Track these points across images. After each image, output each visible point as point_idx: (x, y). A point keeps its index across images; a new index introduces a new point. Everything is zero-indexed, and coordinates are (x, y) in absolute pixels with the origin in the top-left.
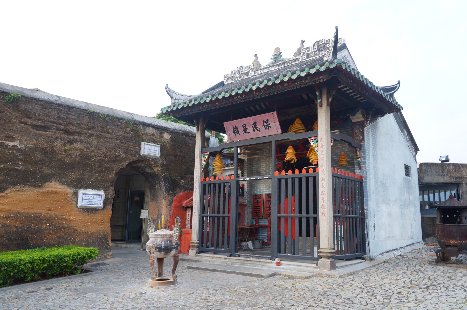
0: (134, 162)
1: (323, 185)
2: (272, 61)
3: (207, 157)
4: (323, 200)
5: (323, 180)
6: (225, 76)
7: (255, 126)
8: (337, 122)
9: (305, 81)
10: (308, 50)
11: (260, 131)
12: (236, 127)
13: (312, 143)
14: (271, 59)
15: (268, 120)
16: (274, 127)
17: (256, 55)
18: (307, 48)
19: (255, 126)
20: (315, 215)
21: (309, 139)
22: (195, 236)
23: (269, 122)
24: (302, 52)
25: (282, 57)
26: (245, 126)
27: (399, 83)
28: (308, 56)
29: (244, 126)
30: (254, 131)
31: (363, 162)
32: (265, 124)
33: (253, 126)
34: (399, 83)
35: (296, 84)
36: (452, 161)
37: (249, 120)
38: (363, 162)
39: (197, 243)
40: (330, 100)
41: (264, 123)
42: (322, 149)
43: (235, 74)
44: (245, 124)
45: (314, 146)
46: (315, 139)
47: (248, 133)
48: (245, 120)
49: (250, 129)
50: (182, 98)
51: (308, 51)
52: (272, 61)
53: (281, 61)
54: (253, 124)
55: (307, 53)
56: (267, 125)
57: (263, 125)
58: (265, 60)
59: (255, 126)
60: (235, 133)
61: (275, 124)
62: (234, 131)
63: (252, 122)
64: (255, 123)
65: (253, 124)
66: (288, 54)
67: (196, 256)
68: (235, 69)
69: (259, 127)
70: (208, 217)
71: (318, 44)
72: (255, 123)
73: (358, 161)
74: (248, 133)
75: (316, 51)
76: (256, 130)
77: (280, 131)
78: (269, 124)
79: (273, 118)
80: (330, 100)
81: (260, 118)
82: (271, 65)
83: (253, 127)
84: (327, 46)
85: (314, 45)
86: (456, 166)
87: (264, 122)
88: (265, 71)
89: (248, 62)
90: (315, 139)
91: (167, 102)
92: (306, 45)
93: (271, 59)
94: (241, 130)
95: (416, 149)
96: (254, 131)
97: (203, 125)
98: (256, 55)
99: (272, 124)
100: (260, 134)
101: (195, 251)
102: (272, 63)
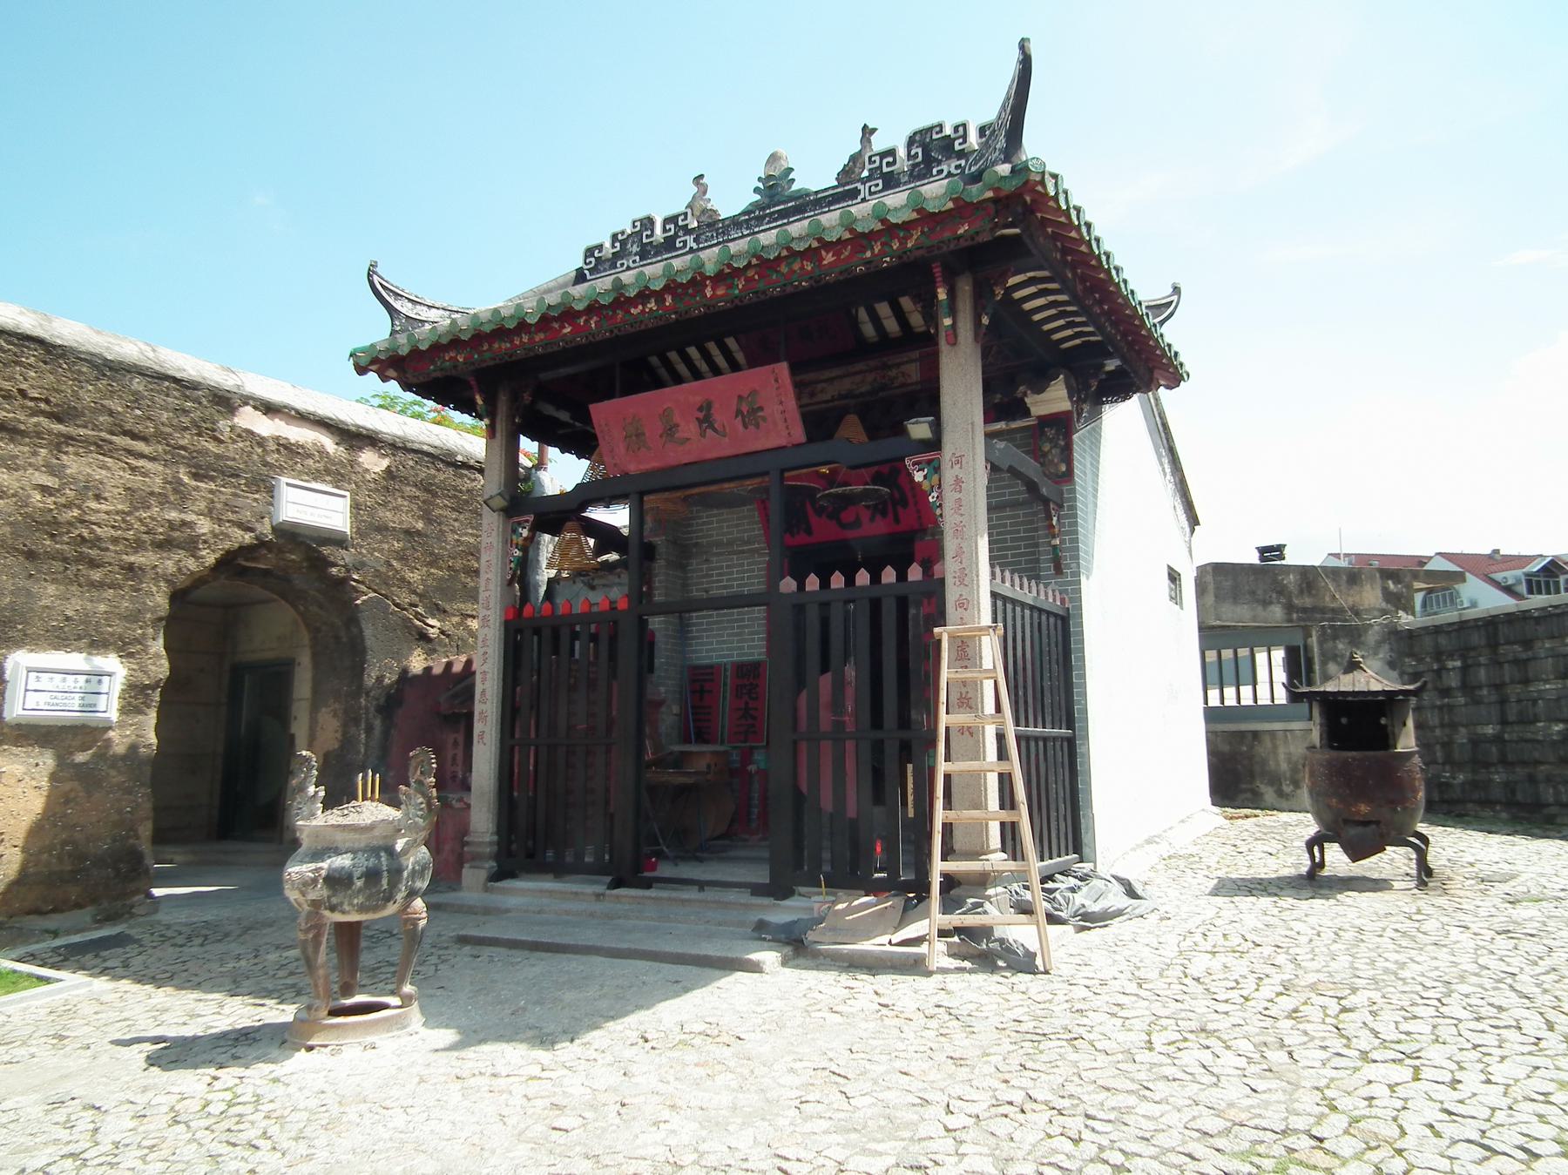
0: (244, 550)
2: (758, 197)
6: (589, 252)
7: (706, 420)
8: (1002, 403)
9: (903, 241)
13: (918, 477)
14: (756, 190)
17: (701, 176)
18: (883, 155)
20: (905, 735)
21: (907, 462)
22: (482, 821)
24: (868, 166)
25: (795, 187)
27: (1176, 290)
30: (703, 435)
31: (1069, 550)
32: (745, 408)
33: (701, 415)
34: (1176, 290)
35: (868, 254)
36: (1292, 558)
38: (1069, 550)
39: (490, 843)
40: (985, 320)
42: (958, 495)
45: (926, 486)
51: (888, 164)
52: (758, 197)
53: (791, 199)
54: (700, 409)
55: (885, 169)
56: (751, 415)
57: (739, 412)
58: (733, 196)
63: (698, 399)
65: (700, 409)
66: (815, 173)
67: (486, 890)
69: (719, 418)
72: (706, 408)
73: (1055, 547)
77: (799, 435)
78: (761, 409)
80: (985, 320)
81: (723, 389)
83: (700, 422)
84: (957, 147)
85: (911, 142)
86: (1308, 576)
90: (929, 462)
91: (376, 330)
92: (879, 144)
93: (756, 190)
95: (1194, 521)
96: (703, 435)
97: (511, 417)
98: (701, 176)
101: (483, 875)
102: (756, 205)
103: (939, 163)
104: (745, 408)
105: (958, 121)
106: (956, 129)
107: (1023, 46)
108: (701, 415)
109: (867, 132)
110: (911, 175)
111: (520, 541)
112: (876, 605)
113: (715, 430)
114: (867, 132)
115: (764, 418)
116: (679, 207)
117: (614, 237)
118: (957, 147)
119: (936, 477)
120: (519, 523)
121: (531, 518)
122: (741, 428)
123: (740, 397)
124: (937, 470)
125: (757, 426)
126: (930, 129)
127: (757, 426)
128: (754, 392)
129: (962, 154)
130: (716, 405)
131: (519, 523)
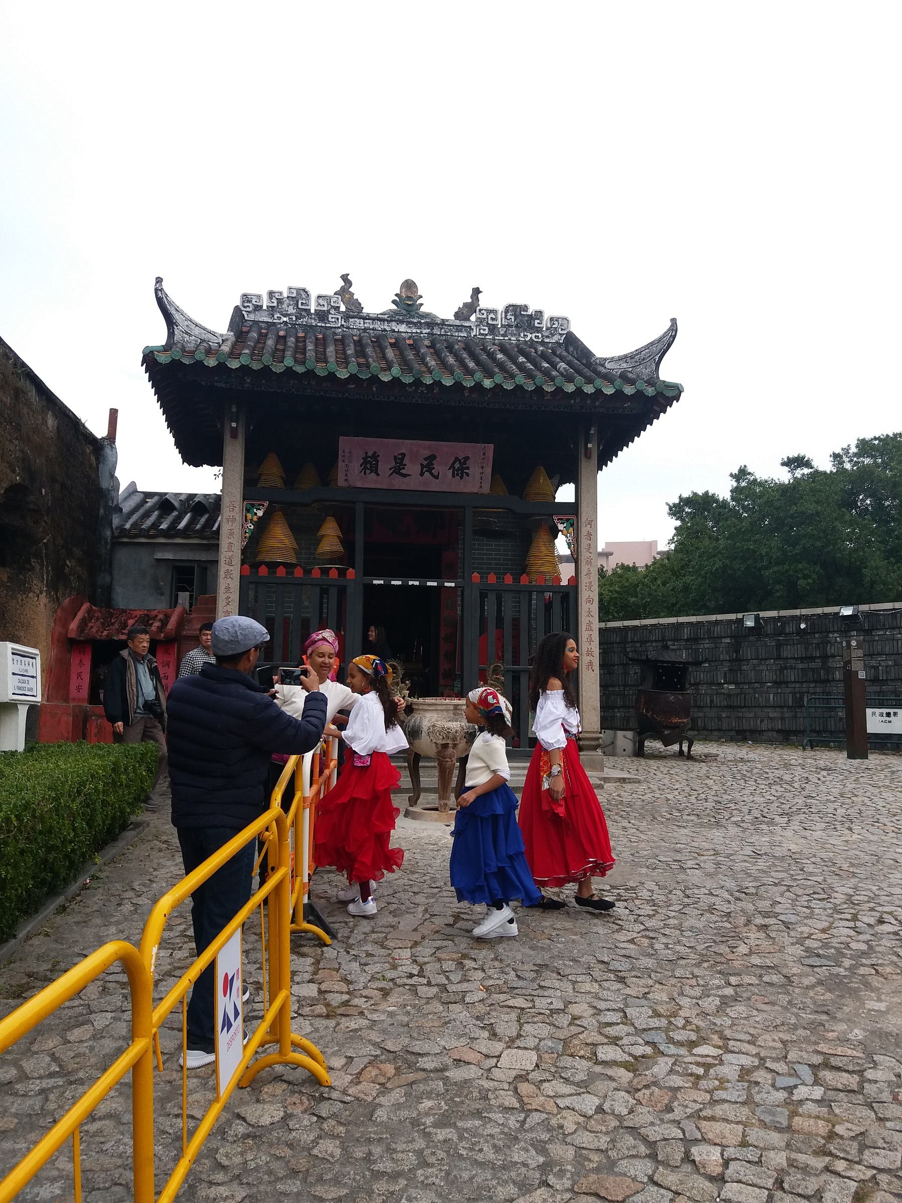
1: (589, 612)
3: (260, 513)
4: (590, 641)
5: (590, 601)
6: (246, 298)
7: (428, 465)
10: (492, 315)
11: (437, 477)
12: (375, 456)
15: (468, 458)
18: (490, 311)
25: (422, 309)
26: (402, 459)
28: (493, 329)
30: (422, 474)
32: (457, 466)
33: (425, 463)
41: (454, 463)
43: (280, 301)
44: (403, 455)
46: (568, 520)
47: (405, 476)
48: (406, 446)
49: (412, 469)
50: (197, 331)
52: (394, 307)
55: (490, 322)
56: (460, 469)
57: (452, 467)
58: (377, 300)
59: (428, 465)
60: (365, 469)
63: (427, 453)
64: (432, 458)
68: (282, 288)
69: (438, 468)
71: (515, 310)
72: (432, 458)
74: (405, 476)
78: (468, 468)
82: (391, 317)
84: (536, 325)
85: (507, 311)
87: (457, 459)
88: (369, 324)
89: (322, 285)
90: (568, 520)
93: (394, 302)
96: (422, 474)
99: (474, 470)
100: (435, 486)
104: (457, 466)
105: (538, 309)
107: (674, 321)
108: (425, 463)
109: (476, 292)
111: (255, 518)
113: (432, 474)
114: (476, 292)
115: (468, 475)
116: (331, 293)
117: (271, 294)
121: (266, 504)
123: (457, 459)
125: (462, 478)
127: (462, 478)
131: (253, 506)
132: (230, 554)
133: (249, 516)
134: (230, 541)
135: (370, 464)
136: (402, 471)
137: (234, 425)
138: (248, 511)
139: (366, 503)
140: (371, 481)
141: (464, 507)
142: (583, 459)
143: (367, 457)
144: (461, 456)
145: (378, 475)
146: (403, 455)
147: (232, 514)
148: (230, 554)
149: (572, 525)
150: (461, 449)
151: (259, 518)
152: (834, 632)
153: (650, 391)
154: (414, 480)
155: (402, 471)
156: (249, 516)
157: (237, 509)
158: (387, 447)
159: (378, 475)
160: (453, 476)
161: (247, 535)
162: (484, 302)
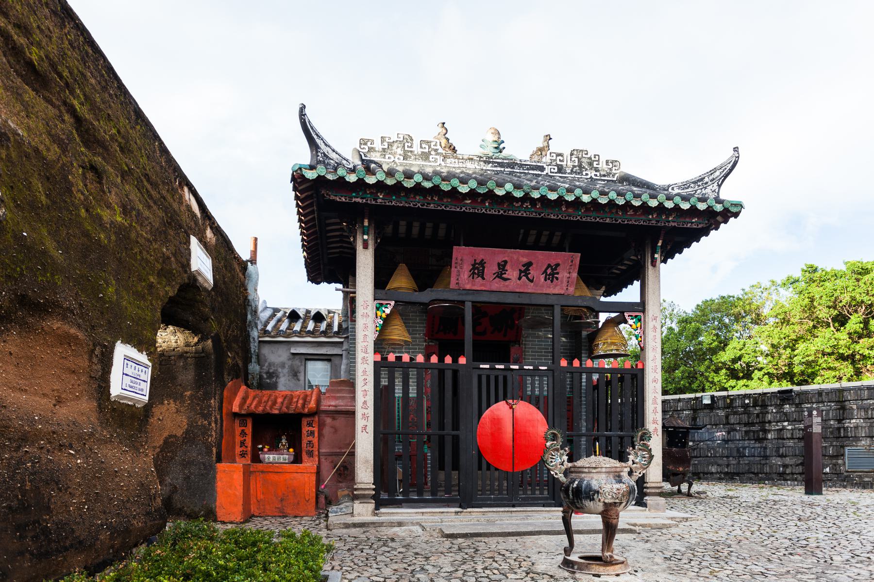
3: (388, 311)
7: (525, 271)
11: (532, 281)
12: (482, 263)
15: (558, 265)
16: (565, 279)
18: (558, 155)
19: (527, 269)
21: (626, 314)
23: (559, 269)
26: (504, 266)
28: (561, 169)
29: (502, 266)
30: (520, 279)
37: (518, 256)
44: (506, 262)
47: (506, 279)
49: (512, 274)
54: (524, 266)
55: (559, 163)
56: (551, 274)
57: (545, 272)
59: (525, 271)
60: (474, 273)
61: (568, 275)
62: (474, 268)
63: (525, 260)
64: (529, 265)
65: (524, 266)
69: (533, 273)
70: (584, 439)
72: (529, 265)
74: (506, 279)
75: (574, 166)
76: (524, 278)
78: (558, 273)
79: (569, 265)
81: (542, 258)
84: (595, 166)
85: (572, 154)
87: (549, 266)
90: (636, 316)
94: (491, 269)
96: (520, 279)
99: (563, 275)
100: (530, 288)
103: (586, 170)
106: (595, 156)
110: (572, 170)
111: (384, 316)
112: (441, 372)
115: (557, 279)
118: (595, 166)
119: (639, 324)
120: (381, 304)
121: (393, 303)
122: (543, 280)
123: (549, 266)
124: (640, 320)
125: (552, 281)
126: (582, 151)
127: (552, 281)
128: (558, 265)
129: (597, 170)
130: (534, 266)
131: (381, 304)
132: (365, 344)
133: (379, 313)
134: (366, 333)
135: (478, 269)
136: (504, 276)
137: (366, 237)
138: (378, 309)
139: (473, 302)
140: (478, 284)
141: (553, 306)
142: (650, 267)
143: (475, 264)
144: (553, 263)
145: (484, 279)
146: (506, 262)
147: (365, 311)
148: (365, 344)
149: (640, 320)
150: (554, 257)
151: (387, 315)
152: (771, 405)
153: (719, 208)
154: (513, 281)
155: (504, 276)
156: (379, 313)
157: (370, 308)
158: (492, 256)
159: (484, 279)
160: (545, 280)
161: (378, 329)
162: (554, 147)
